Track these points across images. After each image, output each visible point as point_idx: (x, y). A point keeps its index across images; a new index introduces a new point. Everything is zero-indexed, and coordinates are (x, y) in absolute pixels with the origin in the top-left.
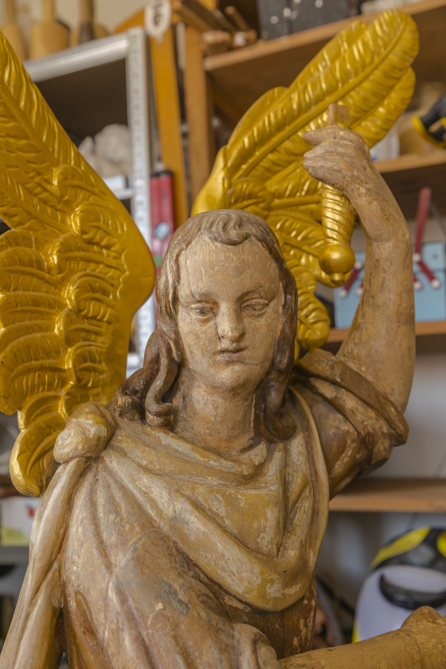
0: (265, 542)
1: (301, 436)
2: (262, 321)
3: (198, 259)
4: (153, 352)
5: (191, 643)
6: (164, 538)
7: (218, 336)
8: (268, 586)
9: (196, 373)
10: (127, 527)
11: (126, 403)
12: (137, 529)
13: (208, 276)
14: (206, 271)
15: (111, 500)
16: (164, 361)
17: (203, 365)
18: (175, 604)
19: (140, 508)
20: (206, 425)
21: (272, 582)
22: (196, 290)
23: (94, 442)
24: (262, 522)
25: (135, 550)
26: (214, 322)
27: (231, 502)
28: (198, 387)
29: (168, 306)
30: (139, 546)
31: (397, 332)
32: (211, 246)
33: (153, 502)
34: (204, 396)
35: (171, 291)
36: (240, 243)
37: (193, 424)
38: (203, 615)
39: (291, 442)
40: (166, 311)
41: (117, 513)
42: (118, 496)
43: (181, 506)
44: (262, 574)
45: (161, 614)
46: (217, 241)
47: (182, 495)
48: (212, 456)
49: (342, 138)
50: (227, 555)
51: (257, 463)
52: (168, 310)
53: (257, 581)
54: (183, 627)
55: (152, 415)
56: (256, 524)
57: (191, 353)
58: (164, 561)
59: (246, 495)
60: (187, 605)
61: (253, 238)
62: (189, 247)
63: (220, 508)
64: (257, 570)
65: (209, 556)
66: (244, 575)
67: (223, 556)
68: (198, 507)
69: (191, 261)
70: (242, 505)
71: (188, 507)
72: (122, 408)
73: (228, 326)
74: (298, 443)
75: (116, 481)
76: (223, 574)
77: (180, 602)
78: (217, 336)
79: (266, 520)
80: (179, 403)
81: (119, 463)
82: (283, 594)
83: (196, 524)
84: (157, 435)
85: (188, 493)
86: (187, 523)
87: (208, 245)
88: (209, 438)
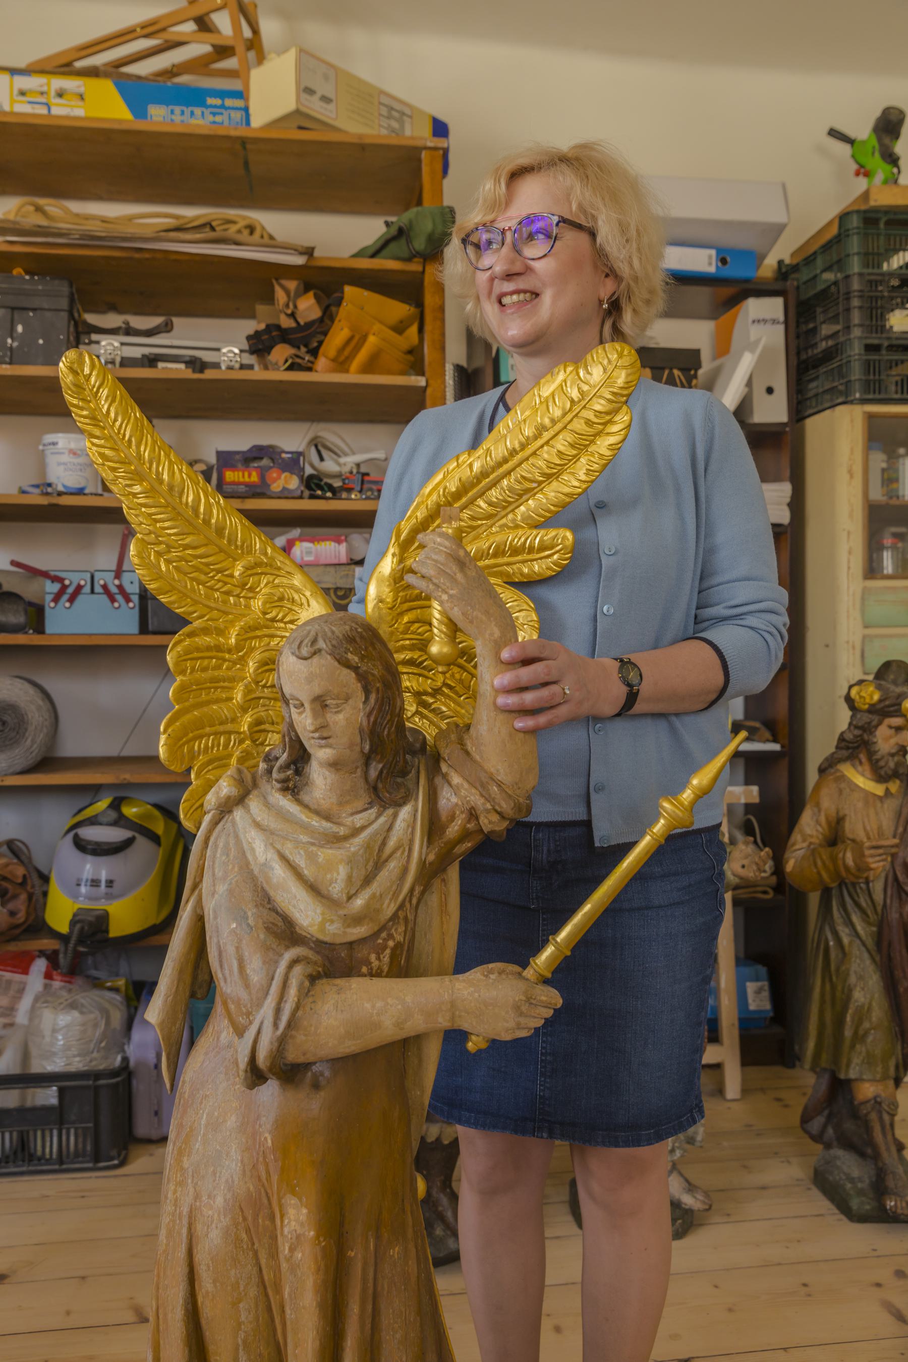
0: (336, 891)
2: (341, 716)
5: (247, 954)
6: (253, 878)
8: (328, 924)
10: (230, 867)
12: (236, 869)
15: (227, 844)
18: (244, 926)
19: (244, 853)
21: (332, 922)
23: (223, 800)
24: (335, 875)
25: (230, 884)
27: (311, 857)
30: (233, 882)
31: (495, 720)
33: (253, 850)
36: (309, 658)
38: (262, 936)
41: (228, 855)
42: (232, 842)
43: (271, 855)
44: (323, 914)
45: (233, 931)
47: (274, 847)
48: (316, 818)
49: (439, 544)
50: (298, 897)
51: (358, 826)
53: (319, 919)
54: (244, 942)
56: (329, 876)
58: (248, 895)
59: (324, 854)
60: (252, 928)
61: (323, 652)
63: (301, 861)
64: (319, 911)
65: (285, 895)
66: (309, 913)
67: (296, 897)
68: (283, 858)
70: (320, 860)
71: (276, 857)
75: (235, 832)
76: (293, 910)
77: (248, 925)
79: (338, 874)
81: (241, 817)
82: (344, 932)
83: (279, 872)
85: (279, 847)
86: (273, 869)
88: (322, 801)
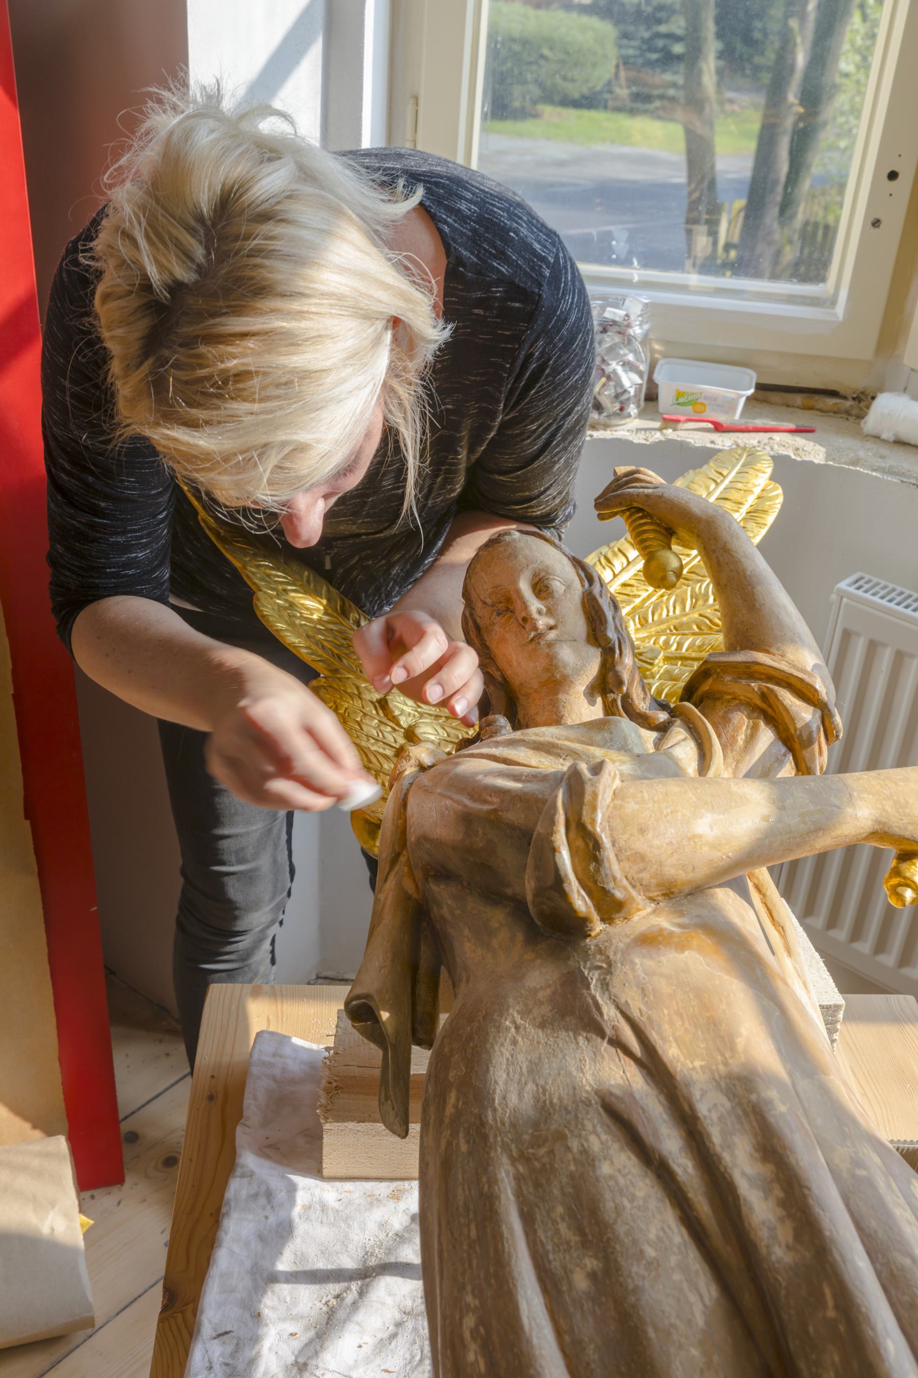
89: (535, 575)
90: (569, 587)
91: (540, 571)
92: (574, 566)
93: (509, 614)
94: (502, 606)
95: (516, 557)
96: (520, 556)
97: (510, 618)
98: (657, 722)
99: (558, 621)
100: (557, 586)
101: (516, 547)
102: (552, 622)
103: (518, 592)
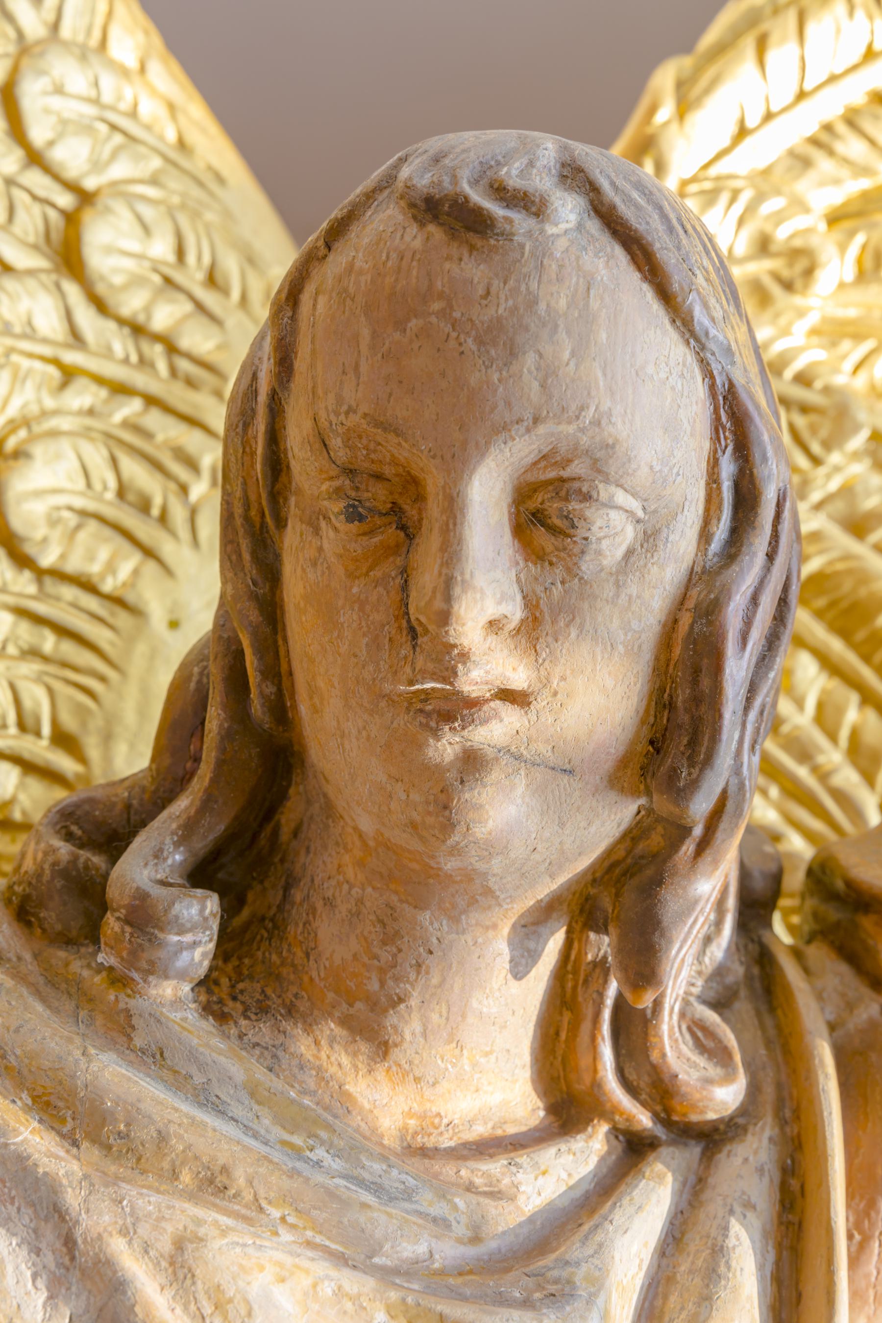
1: (767, 1133)
3: (352, 290)
4: (193, 686)
7: (409, 621)
9: (327, 781)
11: (46, 866)
13: (380, 355)
14: (375, 335)
16: (215, 719)
17: (346, 742)
20: (345, 1005)
22: (333, 417)
26: (399, 561)
28: (337, 844)
29: (253, 497)
32: (407, 238)
34: (351, 886)
35: (260, 426)
37: (296, 995)
39: (720, 1151)
40: (247, 518)
46: (436, 218)
52: (253, 513)
55: (118, 919)
57: (313, 691)
62: (337, 246)
69: (331, 298)
72: (30, 884)
73: (436, 571)
74: (746, 1160)
78: (404, 624)
80: (269, 907)
84: (122, 1005)
87: (399, 235)
89: (546, 458)
90: (650, 537)
91: (576, 452)
92: (717, 425)
93: (392, 534)
94: (378, 495)
95: (513, 352)
96: (530, 360)
97: (393, 550)
98: (694, 1118)
99: (546, 683)
100: (611, 529)
101: (532, 303)
102: (519, 677)
103: (454, 508)
